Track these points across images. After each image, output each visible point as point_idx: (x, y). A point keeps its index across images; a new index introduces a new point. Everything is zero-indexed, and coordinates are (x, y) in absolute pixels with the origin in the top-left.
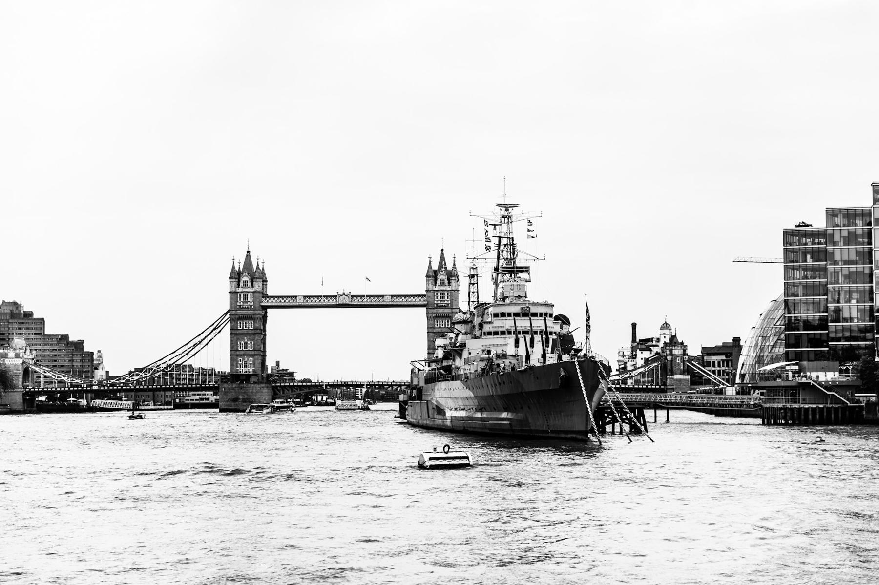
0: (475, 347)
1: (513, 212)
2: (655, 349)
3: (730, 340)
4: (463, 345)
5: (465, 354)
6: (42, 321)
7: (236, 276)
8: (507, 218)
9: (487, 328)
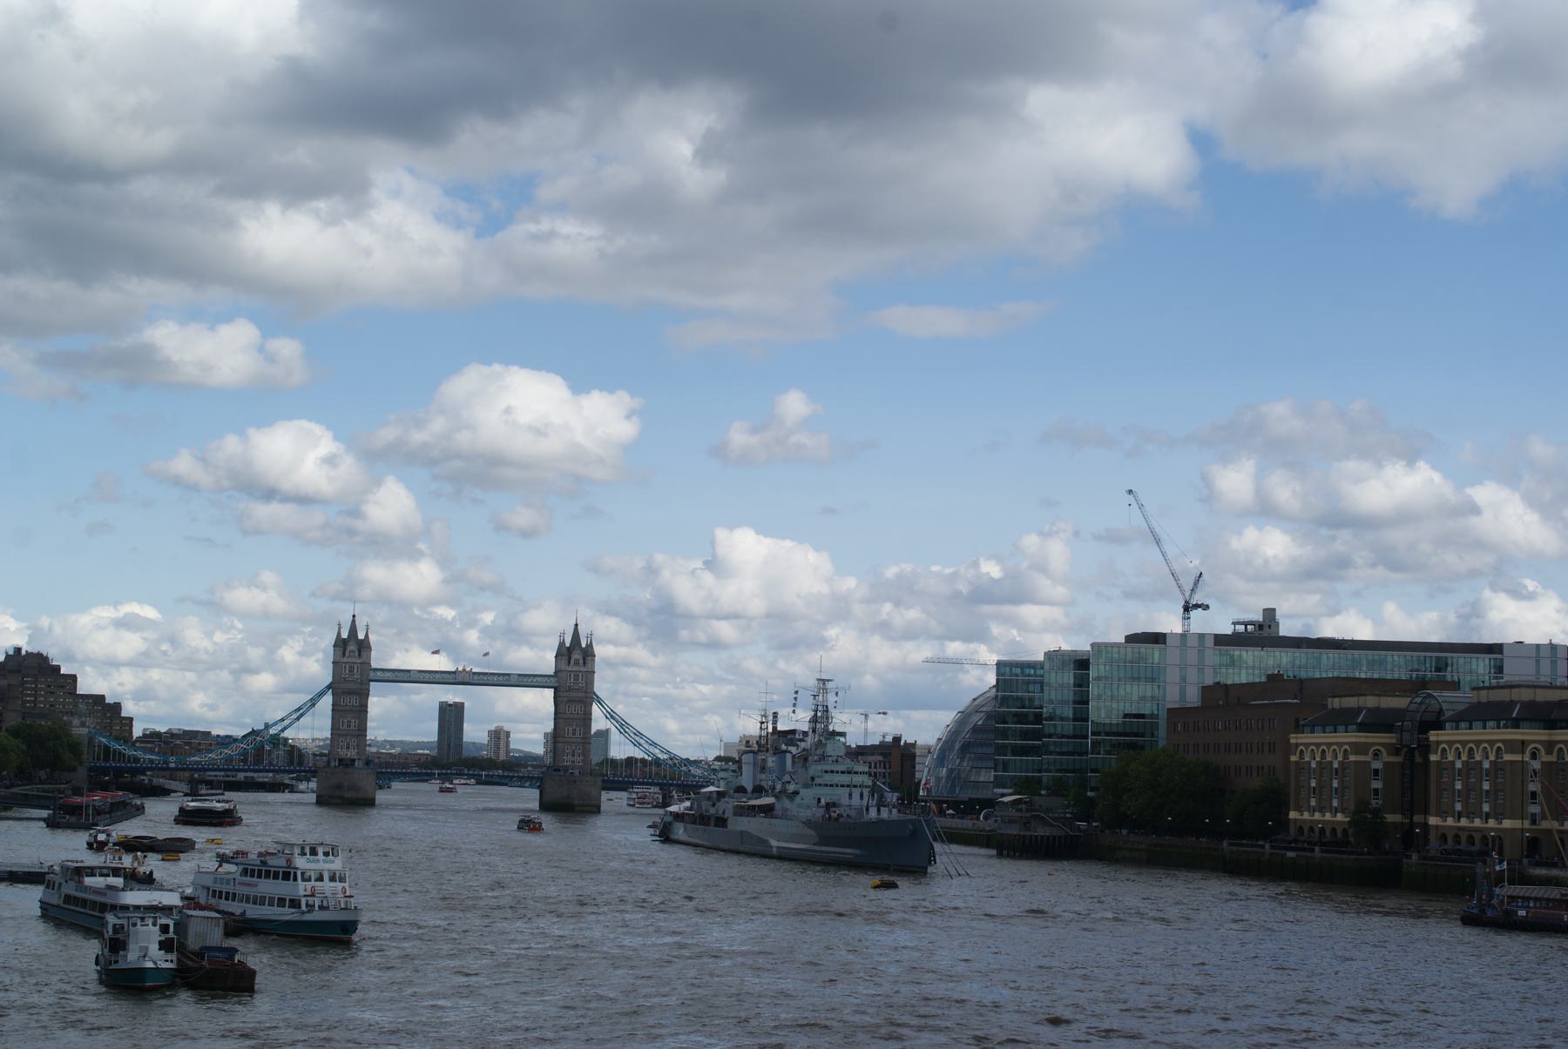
0: (808, 795)
1: (829, 685)
2: (802, 745)
3: (889, 739)
4: (796, 793)
5: (798, 799)
6: (74, 678)
7: (341, 644)
8: (825, 691)
9: (818, 781)
